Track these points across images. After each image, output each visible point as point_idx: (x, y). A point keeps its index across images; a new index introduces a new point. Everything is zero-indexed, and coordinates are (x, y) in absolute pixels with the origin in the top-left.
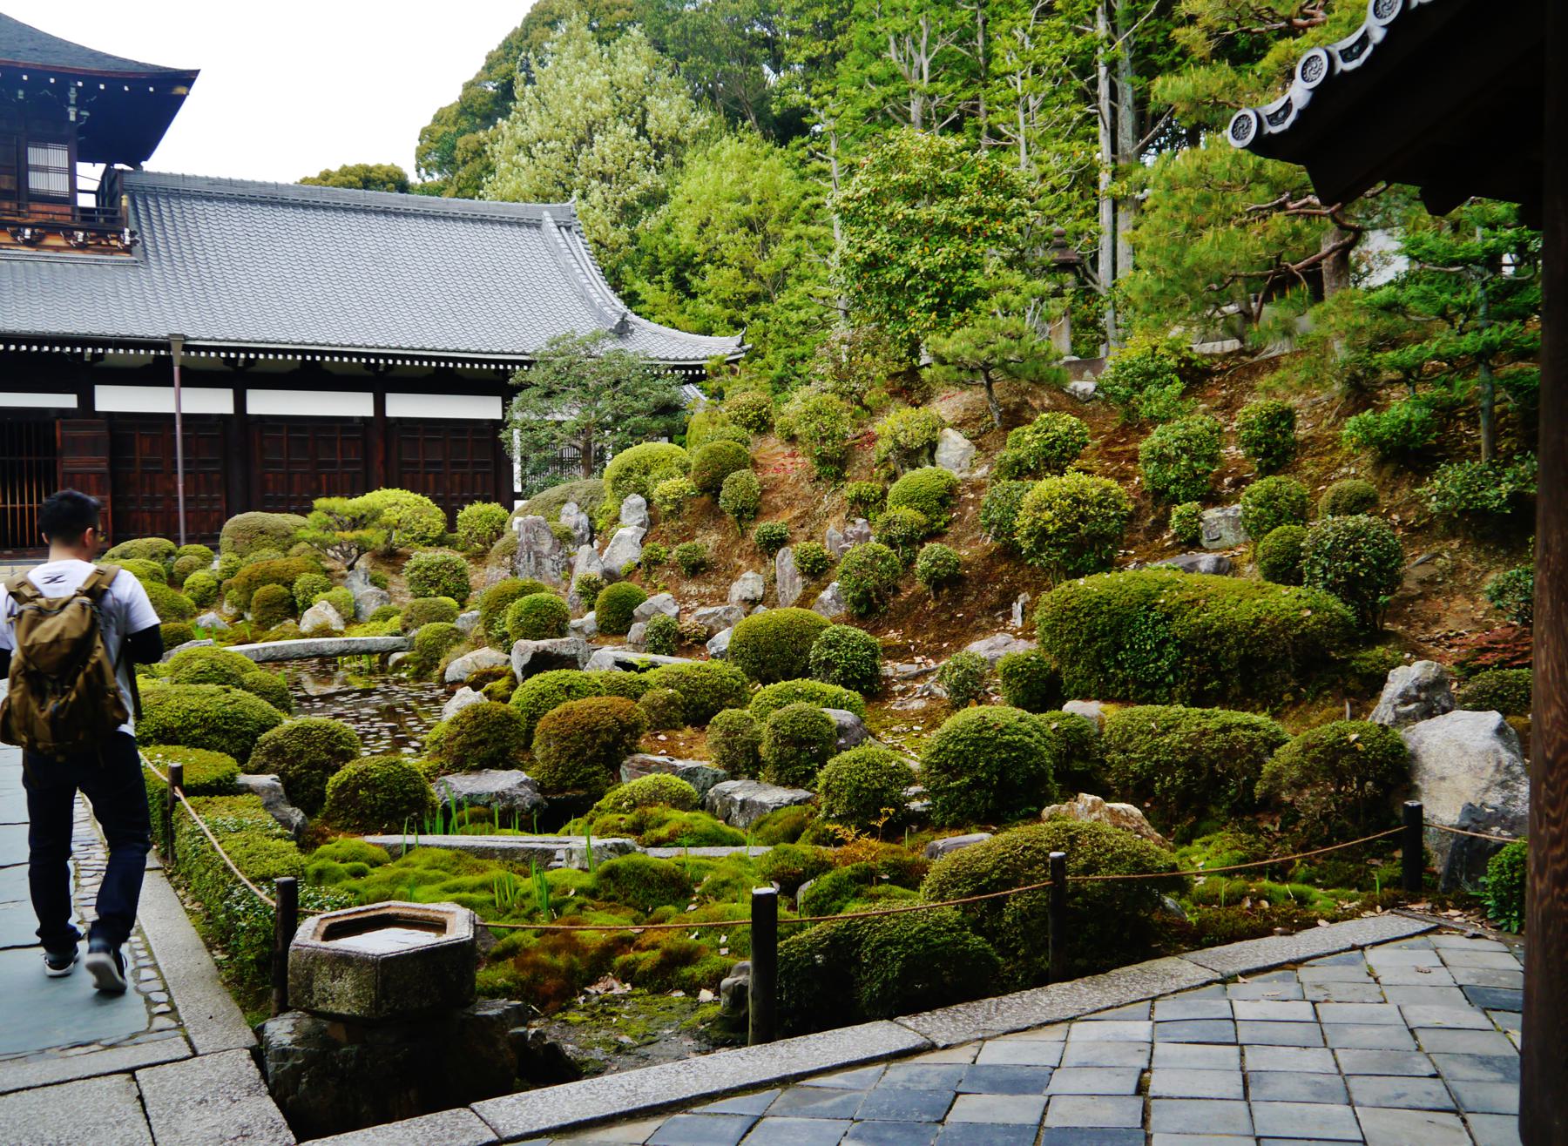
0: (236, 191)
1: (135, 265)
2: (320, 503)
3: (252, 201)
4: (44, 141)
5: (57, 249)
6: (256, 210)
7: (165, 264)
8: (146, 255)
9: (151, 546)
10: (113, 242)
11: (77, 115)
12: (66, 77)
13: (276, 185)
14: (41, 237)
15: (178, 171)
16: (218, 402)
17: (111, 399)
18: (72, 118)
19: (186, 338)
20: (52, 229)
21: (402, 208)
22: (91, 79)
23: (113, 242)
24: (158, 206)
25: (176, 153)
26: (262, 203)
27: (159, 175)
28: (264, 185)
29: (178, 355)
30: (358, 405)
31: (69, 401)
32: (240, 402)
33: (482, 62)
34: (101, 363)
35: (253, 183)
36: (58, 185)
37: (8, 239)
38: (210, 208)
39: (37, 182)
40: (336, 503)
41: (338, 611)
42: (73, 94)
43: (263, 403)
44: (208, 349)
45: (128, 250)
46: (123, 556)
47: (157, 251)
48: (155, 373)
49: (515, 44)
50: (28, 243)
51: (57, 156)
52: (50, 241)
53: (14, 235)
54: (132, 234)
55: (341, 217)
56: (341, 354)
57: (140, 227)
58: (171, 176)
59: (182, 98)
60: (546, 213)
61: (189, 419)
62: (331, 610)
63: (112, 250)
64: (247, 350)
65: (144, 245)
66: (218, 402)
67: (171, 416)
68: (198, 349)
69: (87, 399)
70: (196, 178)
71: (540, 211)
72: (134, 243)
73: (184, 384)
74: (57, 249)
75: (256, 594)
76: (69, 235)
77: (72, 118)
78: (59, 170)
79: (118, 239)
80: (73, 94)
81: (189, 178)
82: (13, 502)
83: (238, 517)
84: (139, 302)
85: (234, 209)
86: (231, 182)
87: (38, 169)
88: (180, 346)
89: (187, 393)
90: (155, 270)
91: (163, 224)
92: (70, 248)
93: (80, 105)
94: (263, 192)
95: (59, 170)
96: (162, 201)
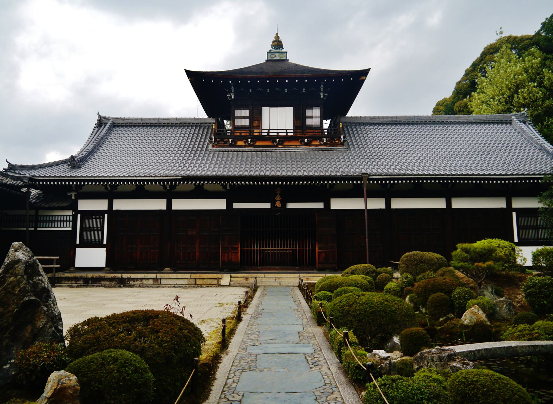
0: (381, 121)
1: (345, 150)
2: (459, 246)
3: (387, 124)
4: (311, 107)
5: (316, 146)
6: (389, 127)
7: (357, 149)
8: (349, 147)
9: (365, 268)
10: (337, 142)
11: (323, 95)
13: (397, 117)
14: (311, 142)
15: (358, 115)
16: (378, 204)
17: (337, 204)
18: (322, 97)
20: (314, 138)
21: (449, 121)
23: (337, 142)
24: (352, 129)
25: (356, 110)
26: (391, 124)
27: (352, 117)
28: (392, 117)
29: (365, 182)
31: (321, 205)
33: (463, 73)
35: (387, 117)
37: (299, 144)
38: (372, 128)
39: (309, 122)
40: (466, 245)
41: (484, 311)
42: (322, 88)
44: (377, 179)
45: (342, 144)
46: (353, 273)
47: (353, 144)
49: (477, 63)
50: (306, 144)
51: (317, 112)
52: (314, 143)
53: (301, 142)
54: (344, 138)
55: (423, 127)
56: (435, 179)
58: (356, 117)
59: (363, 81)
60: (513, 117)
62: (481, 312)
63: (337, 145)
64: (394, 179)
65: (348, 143)
66: (378, 204)
67: (364, 210)
68: (373, 180)
69: (327, 204)
70: (365, 117)
72: (345, 141)
74: (316, 146)
75: (430, 298)
76: (321, 140)
77: (322, 97)
78: (317, 117)
79: (339, 140)
80: (322, 88)
81: (363, 117)
82: (299, 247)
83: (408, 254)
84: (348, 163)
85: (380, 127)
86: (379, 118)
88: (366, 178)
90: (353, 151)
91: (354, 135)
92: (321, 145)
93: (324, 92)
94: (392, 120)
95: (317, 117)
96: (353, 127)
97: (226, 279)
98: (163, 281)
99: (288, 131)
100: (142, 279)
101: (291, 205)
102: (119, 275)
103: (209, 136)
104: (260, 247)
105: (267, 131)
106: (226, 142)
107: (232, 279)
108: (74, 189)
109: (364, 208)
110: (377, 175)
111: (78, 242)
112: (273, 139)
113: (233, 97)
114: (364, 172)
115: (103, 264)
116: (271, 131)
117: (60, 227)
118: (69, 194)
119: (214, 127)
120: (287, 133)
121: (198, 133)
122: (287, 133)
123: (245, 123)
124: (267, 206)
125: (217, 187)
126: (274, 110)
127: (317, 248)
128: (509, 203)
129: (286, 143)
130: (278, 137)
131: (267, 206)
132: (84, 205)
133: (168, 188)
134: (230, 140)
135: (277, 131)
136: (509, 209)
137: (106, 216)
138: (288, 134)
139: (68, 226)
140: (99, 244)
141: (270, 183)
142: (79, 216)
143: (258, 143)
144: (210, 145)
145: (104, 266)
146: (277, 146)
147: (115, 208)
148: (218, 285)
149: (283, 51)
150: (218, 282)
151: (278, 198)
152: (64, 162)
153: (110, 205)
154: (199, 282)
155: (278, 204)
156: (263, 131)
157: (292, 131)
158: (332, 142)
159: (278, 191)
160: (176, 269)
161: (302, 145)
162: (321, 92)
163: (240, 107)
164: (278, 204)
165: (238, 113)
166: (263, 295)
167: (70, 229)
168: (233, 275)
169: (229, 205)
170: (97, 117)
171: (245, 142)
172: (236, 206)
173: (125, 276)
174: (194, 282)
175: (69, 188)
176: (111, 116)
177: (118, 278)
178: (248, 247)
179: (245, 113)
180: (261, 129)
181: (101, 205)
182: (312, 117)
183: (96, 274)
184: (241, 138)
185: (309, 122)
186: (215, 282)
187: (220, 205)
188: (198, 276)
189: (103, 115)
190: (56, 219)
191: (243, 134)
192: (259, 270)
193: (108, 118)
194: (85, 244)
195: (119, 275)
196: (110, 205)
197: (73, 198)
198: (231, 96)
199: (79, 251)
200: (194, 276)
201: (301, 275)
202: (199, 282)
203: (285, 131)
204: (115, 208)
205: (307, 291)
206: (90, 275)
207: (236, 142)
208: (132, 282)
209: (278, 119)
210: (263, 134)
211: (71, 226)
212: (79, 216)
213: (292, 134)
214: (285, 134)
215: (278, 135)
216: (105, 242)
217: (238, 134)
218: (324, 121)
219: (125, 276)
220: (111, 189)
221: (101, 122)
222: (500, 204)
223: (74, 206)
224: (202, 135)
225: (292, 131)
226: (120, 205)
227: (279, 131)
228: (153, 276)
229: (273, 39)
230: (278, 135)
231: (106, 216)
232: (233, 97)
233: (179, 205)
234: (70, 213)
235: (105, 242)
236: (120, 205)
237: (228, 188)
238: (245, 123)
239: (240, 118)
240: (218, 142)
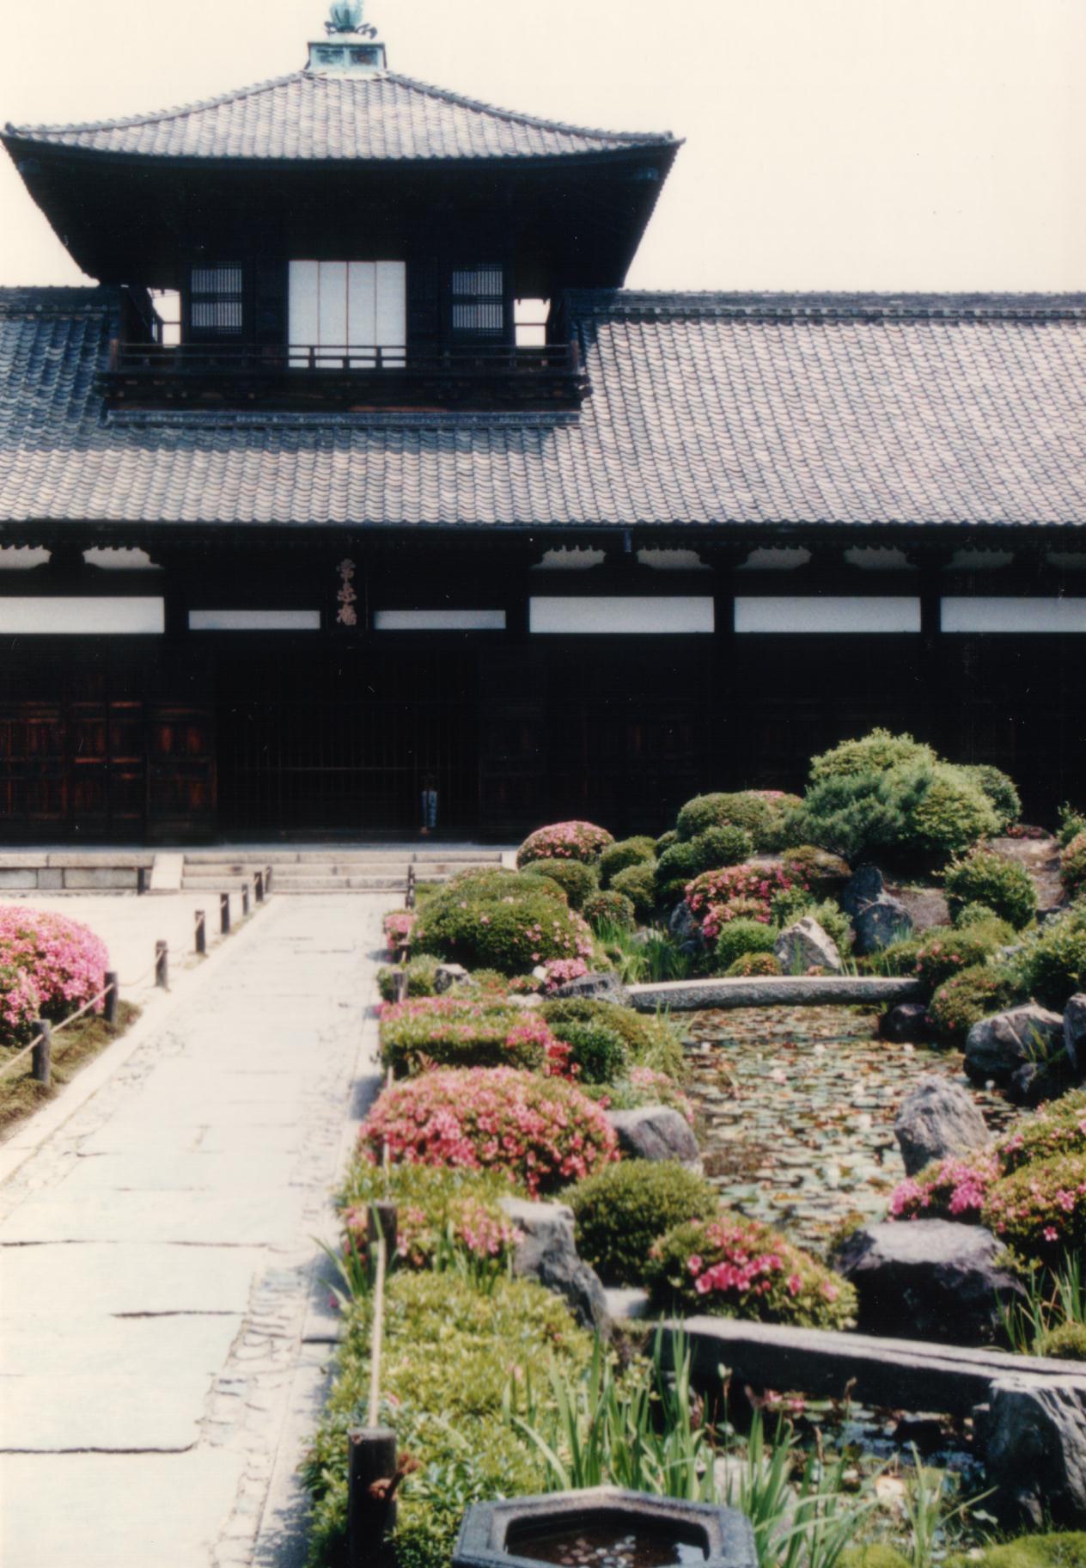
17: (552, 616)
23: (558, 393)
31: (494, 620)
32: (724, 615)
36: (488, 318)
39: (464, 318)
51: (490, 282)
69: (519, 617)
95: (488, 300)
97: (167, 865)
99: (385, 353)
101: (393, 620)
105: (306, 352)
107: (191, 868)
116: (324, 352)
120: (379, 359)
122: (379, 359)
123: (230, 316)
124: (308, 620)
131: (308, 620)
135: (342, 352)
138: (386, 364)
148: (142, 887)
151: (346, 594)
154: (73, 879)
155: (347, 615)
157: (402, 353)
164: (347, 615)
165: (200, 282)
169: (175, 616)
172: (201, 620)
174: (58, 882)
179: (230, 280)
182: (472, 300)
185: (464, 318)
187: (141, 616)
202: (73, 879)
203: (372, 352)
205: (412, 887)
209: (347, 311)
210: (293, 363)
213: (401, 364)
214: (371, 364)
227: (352, 352)
238: (230, 316)
239: (211, 298)
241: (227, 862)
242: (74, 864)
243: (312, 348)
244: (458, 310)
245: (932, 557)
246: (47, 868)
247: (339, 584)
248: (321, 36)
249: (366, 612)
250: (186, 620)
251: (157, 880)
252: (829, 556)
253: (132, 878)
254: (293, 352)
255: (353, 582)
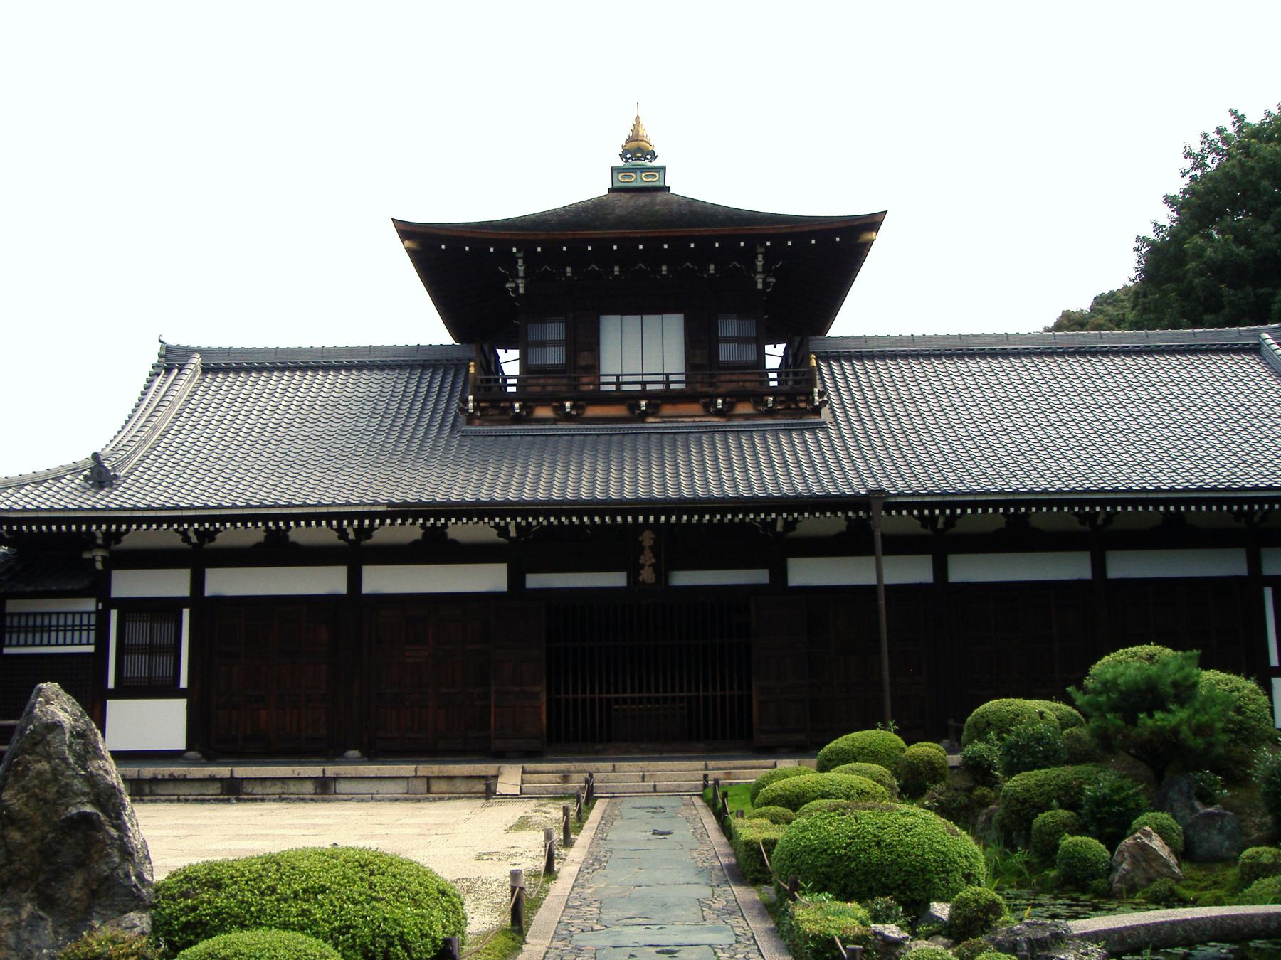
5: (746, 417)
11: (765, 283)
12: (755, 240)
15: (859, 333)
16: (912, 571)
17: (805, 573)
18: (760, 286)
19: (889, 495)
20: (743, 396)
22: (779, 238)
23: (802, 405)
25: (856, 318)
30: (1070, 567)
31: (760, 576)
32: (940, 569)
34: (792, 534)
39: (729, 353)
43: (968, 570)
48: (855, 541)
50: (719, 414)
54: (821, 394)
57: (824, 386)
59: (867, 246)
61: (893, 589)
65: (832, 407)
66: (912, 571)
68: (899, 507)
69: (779, 573)
71: (1257, 334)
73: (887, 552)
74: (746, 417)
77: (760, 286)
87: (728, 340)
89: (888, 561)
97: (510, 778)
98: (342, 787)
99: (672, 378)
100: (283, 780)
101: (682, 578)
102: (223, 771)
103: (458, 395)
104: (600, 692)
105: (614, 379)
106: (504, 411)
108: (100, 541)
109: (873, 581)
110: (908, 495)
111: (111, 685)
112: (629, 399)
113: (521, 290)
114: (874, 487)
115: (180, 744)
117: (80, 644)
118: (87, 555)
119: (472, 370)
121: (429, 386)
122: (668, 383)
123: (557, 357)
124: (617, 579)
125: (482, 531)
126: (632, 321)
127: (755, 692)
128: (1254, 563)
129: (667, 410)
130: (644, 394)
131: (617, 579)
132: (127, 585)
133: (352, 536)
134: (517, 405)
135: (639, 379)
136: (1255, 580)
137: (186, 613)
138: (673, 386)
139: (84, 641)
140: (167, 689)
141: (625, 519)
142: (114, 614)
143: (592, 411)
144: (463, 418)
145: (180, 744)
146: (642, 417)
147: (209, 591)
149: (656, 163)
150: (488, 786)
151: (647, 558)
152: (75, 470)
153: (198, 583)
155: (647, 575)
156: (603, 379)
157: (682, 378)
158: (789, 408)
159: (647, 538)
160: (373, 754)
161: (709, 414)
162: (756, 273)
163: (542, 316)
164: (647, 575)
165: (535, 332)
166: (606, 820)
167: (91, 649)
168: (530, 766)
169: (516, 578)
170: (157, 348)
171: (555, 409)
172: (535, 581)
173: (241, 772)
174: (424, 789)
175: (88, 541)
176: (194, 345)
177: (221, 780)
178: (567, 692)
179: (557, 330)
180: (599, 376)
181: (175, 584)
183: (164, 770)
184: (543, 400)
185: (729, 353)
186: (481, 787)
188: (435, 769)
189: (171, 342)
190: (54, 622)
191: (549, 389)
192: (597, 752)
193: (188, 352)
194: (131, 689)
195: (223, 771)
196: (198, 583)
197: (99, 566)
198: (516, 289)
199: (115, 707)
200: (425, 770)
201: (711, 764)
204: (209, 591)
206: (148, 771)
207: (531, 411)
208: (258, 789)
209: (644, 350)
210: (603, 388)
211: (92, 639)
212: (114, 614)
213: (682, 386)
214: (660, 387)
215: (644, 389)
216: (184, 683)
217: (538, 389)
218: (769, 349)
219: (241, 772)
220: (199, 540)
221: (171, 360)
222: (1230, 565)
223: (99, 588)
224: (440, 391)
225: (682, 378)
226: (224, 583)
227: (646, 379)
228: (315, 771)
229: (627, 133)
230: (644, 389)
231: (186, 613)
232: (521, 290)
233: (382, 580)
234: (90, 605)
235: (184, 683)
236: (222, 582)
237: (513, 533)
238: (557, 357)
239: (542, 344)
240: (483, 409)
241: (557, 772)
242: (436, 774)
243: (618, 376)
244: (722, 347)
245: (1096, 521)
246: (415, 777)
247: (641, 550)
248: (620, 163)
249: (662, 572)
250: (523, 581)
251: (501, 788)
252: (1019, 521)
253: (481, 787)
254: (603, 379)
255: (655, 549)
